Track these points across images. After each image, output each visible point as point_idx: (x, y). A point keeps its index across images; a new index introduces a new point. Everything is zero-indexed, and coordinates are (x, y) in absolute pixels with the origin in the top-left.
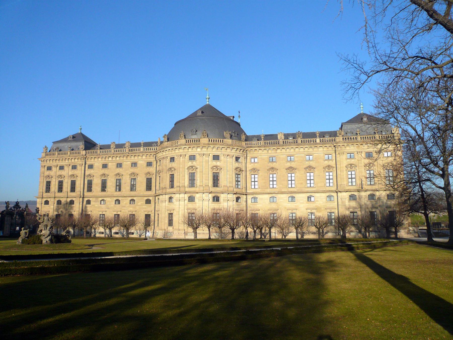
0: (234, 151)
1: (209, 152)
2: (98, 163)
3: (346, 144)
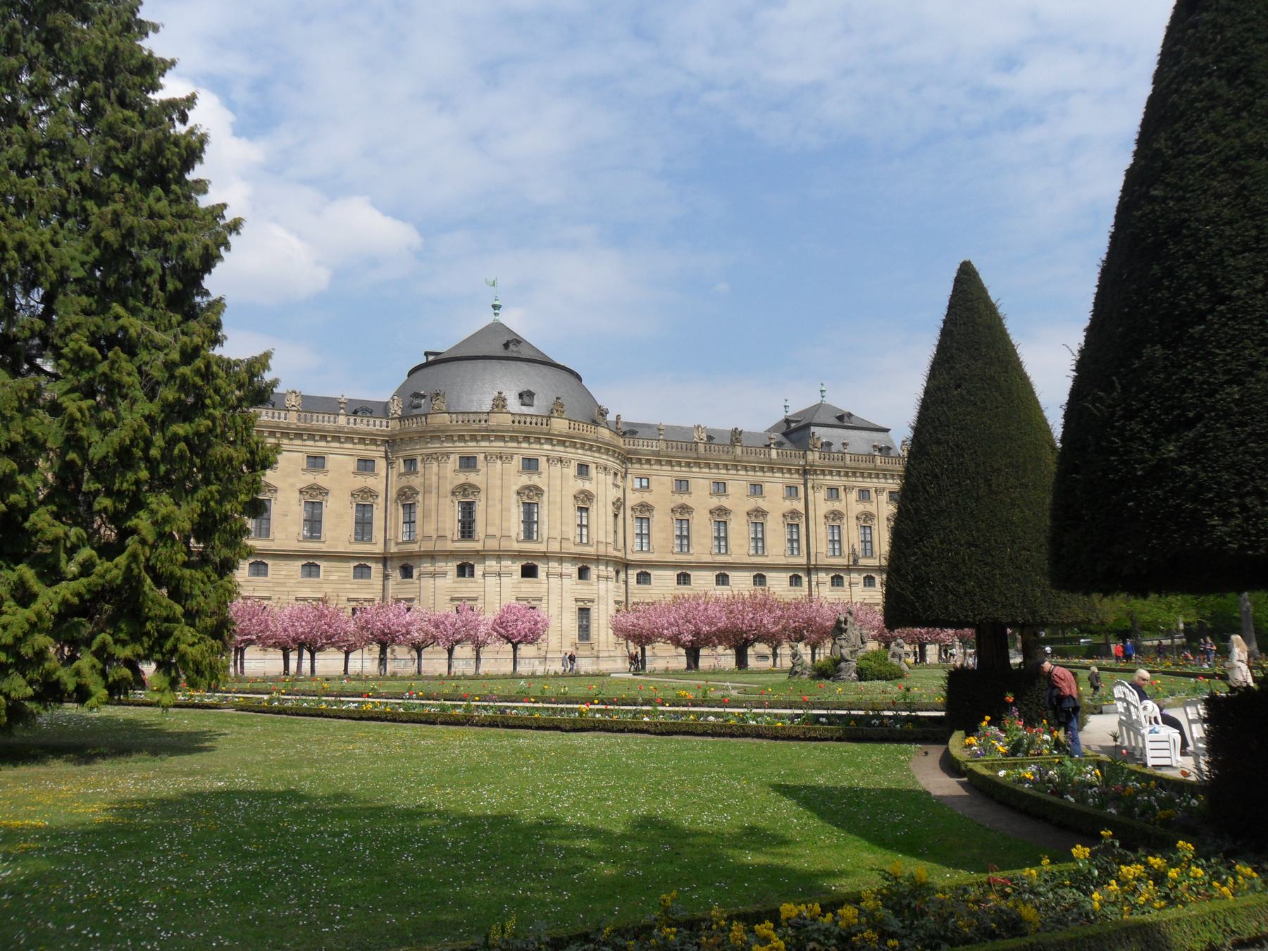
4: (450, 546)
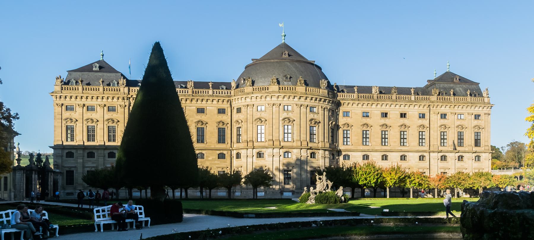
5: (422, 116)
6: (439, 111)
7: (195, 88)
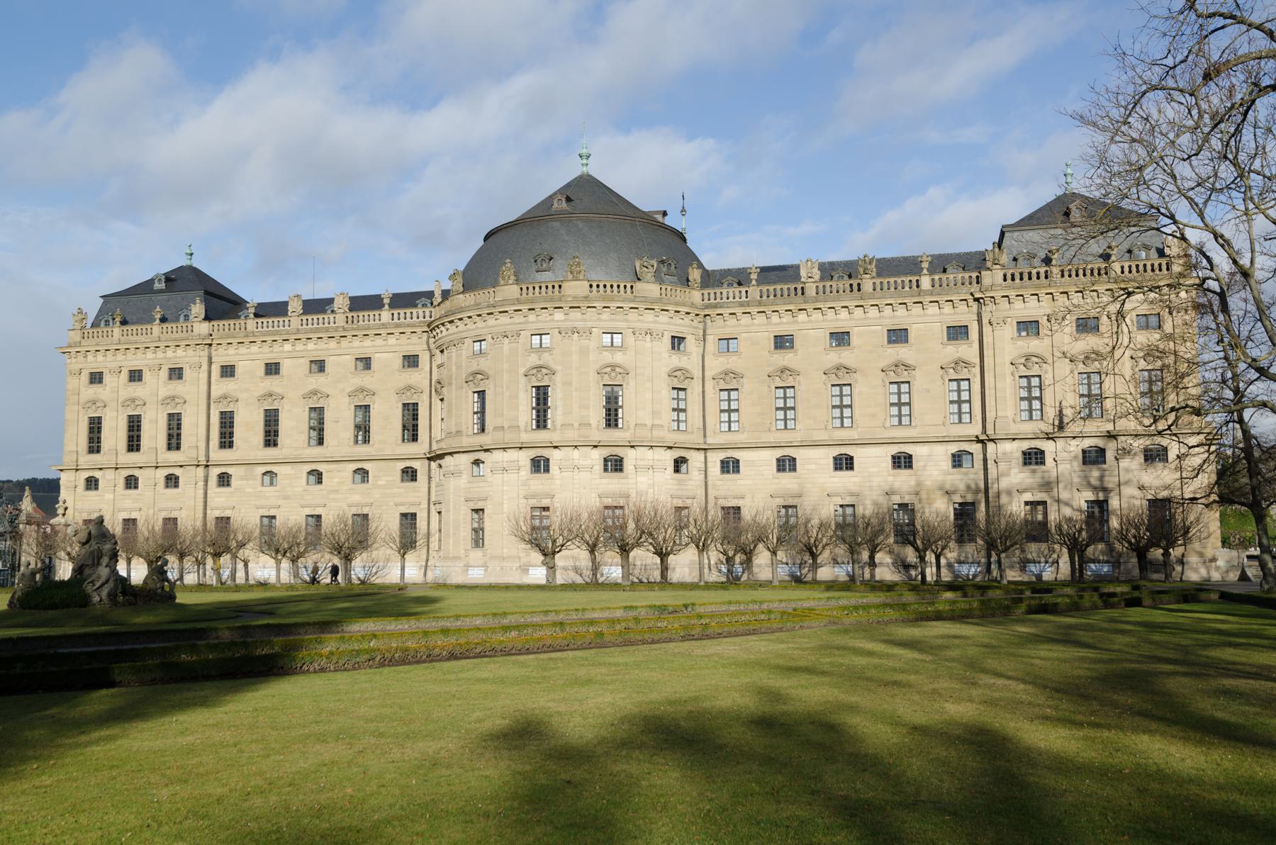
0: (664, 317)
1: (589, 324)
2: (249, 359)
3: (1012, 293)
4: (466, 442)
5: (957, 333)
6: (1011, 313)
7: (351, 310)
